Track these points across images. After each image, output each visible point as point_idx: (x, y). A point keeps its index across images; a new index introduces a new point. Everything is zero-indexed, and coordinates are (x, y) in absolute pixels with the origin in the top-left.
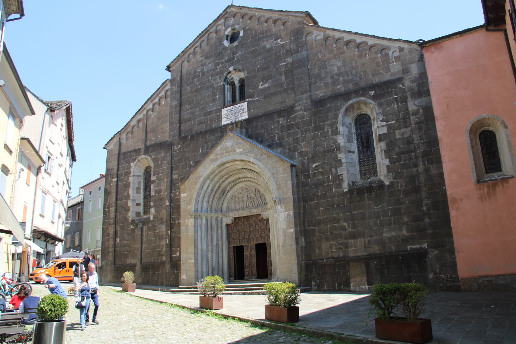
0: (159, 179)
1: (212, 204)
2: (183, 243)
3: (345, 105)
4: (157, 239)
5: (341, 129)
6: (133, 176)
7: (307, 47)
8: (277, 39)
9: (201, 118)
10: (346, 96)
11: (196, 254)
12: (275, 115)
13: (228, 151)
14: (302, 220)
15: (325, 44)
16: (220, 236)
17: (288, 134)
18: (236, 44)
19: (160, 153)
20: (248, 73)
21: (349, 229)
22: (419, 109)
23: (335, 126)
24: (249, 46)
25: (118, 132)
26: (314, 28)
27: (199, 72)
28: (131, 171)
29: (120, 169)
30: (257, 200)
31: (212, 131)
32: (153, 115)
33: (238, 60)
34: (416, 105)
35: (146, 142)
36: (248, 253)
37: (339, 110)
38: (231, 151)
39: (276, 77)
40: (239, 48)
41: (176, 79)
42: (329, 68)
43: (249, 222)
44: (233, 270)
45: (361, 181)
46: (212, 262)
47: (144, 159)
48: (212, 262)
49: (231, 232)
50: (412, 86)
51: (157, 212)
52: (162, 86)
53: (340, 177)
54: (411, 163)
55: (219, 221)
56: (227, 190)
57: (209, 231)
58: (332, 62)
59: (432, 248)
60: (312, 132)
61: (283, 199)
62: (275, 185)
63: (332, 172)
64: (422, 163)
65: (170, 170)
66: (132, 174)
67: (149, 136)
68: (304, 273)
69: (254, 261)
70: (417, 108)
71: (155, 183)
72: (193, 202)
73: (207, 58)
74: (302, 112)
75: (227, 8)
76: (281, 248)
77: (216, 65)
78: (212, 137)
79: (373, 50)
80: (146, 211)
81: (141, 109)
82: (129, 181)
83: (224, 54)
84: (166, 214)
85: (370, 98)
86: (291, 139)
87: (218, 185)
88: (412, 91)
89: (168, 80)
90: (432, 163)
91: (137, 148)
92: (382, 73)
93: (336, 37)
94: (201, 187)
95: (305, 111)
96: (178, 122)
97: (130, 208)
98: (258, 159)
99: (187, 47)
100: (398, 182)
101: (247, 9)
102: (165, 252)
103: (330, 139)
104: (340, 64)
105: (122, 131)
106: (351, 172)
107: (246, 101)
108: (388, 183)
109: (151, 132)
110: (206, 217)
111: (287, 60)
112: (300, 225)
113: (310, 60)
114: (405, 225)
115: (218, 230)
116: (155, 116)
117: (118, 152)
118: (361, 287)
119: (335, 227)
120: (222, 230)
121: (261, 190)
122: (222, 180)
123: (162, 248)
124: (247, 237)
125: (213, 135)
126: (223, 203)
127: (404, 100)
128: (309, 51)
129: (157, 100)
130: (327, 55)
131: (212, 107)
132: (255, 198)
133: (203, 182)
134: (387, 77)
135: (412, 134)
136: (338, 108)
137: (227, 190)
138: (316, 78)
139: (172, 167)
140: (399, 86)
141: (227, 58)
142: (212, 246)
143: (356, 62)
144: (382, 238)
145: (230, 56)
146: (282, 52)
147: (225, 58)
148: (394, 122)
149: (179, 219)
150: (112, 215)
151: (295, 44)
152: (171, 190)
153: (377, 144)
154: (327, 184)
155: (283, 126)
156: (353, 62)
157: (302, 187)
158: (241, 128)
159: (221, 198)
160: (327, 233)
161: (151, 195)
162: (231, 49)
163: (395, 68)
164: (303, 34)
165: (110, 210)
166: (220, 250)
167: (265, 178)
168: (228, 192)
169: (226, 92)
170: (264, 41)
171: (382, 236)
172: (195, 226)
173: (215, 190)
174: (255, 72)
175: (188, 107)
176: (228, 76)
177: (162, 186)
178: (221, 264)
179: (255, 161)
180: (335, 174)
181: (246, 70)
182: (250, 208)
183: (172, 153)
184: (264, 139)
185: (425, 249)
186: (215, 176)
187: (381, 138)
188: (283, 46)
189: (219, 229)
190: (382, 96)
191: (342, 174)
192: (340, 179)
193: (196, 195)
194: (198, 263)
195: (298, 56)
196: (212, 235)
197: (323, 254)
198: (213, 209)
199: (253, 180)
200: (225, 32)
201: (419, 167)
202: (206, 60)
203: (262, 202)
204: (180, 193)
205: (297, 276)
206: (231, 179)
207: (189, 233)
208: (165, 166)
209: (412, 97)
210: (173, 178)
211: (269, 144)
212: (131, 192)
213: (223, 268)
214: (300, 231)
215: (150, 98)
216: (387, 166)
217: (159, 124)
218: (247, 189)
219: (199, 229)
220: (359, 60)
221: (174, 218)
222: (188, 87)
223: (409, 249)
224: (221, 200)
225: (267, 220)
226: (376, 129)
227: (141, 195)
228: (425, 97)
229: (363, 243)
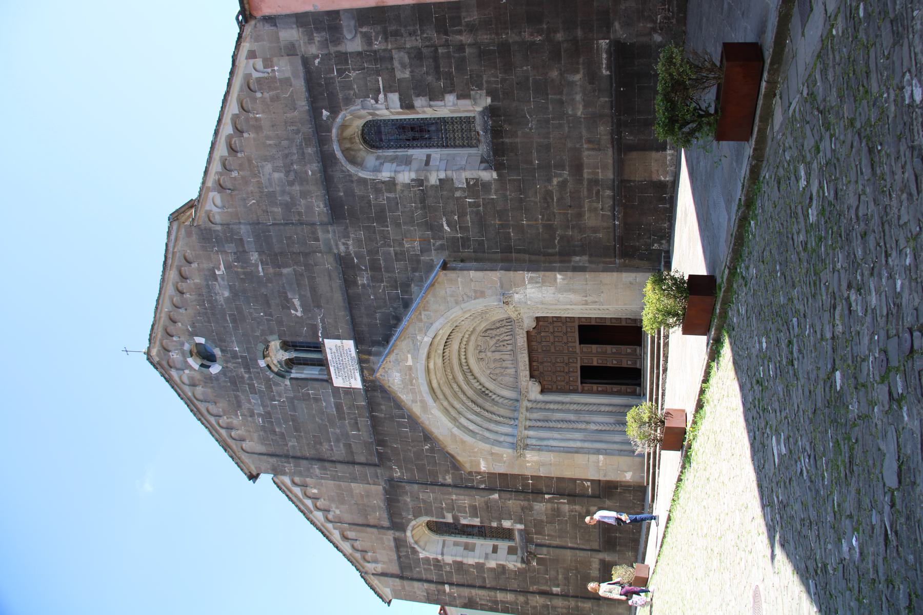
0: (451, 509)
1: (502, 417)
2: (568, 474)
3: (344, 164)
4: (559, 520)
5: (385, 175)
6: (442, 554)
7: (233, 224)
8: (214, 277)
9: (347, 424)
10: (327, 161)
11: (589, 452)
12: (350, 291)
13: (410, 381)
14: (542, 258)
15: (230, 191)
16: (560, 407)
17: (388, 270)
18: (217, 352)
19: (405, 503)
20: (272, 333)
21: (565, 176)
22: (361, 32)
23: (380, 186)
24: (224, 327)
25: (362, 577)
26: (201, 207)
27: (263, 422)
28: (433, 559)
29: (429, 577)
30: (501, 335)
31: (372, 406)
32: (336, 511)
33: (248, 350)
34: (353, 38)
35: (383, 528)
36: (595, 359)
37: (350, 176)
38: (410, 375)
39: (283, 284)
40: (225, 347)
41: (273, 465)
42: (274, 186)
43: (540, 352)
44: (623, 387)
45: (480, 147)
46: (606, 424)
47: (414, 532)
48: (606, 424)
49: (554, 386)
50: (319, 41)
51: (510, 515)
52: (284, 492)
53: (471, 183)
54: (457, 55)
55: (534, 405)
56: (480, 387)
57: (551, 424)
58: (264, 180)
59: (609, 32)
60: (388, 227)
61: (502, 287)
62: (477, 301)
63: (460, 197)
64: (457, 37)
65: (436, 487)
66: (440, 557)
67: (372, 521)
68: (637, 262)
69: (609, 349)
70: (359, 35)
71: (458, 516)
72: (496, 449)
73: (239, 406)
74: (350, 242)
75: (152, 363)
76: (589, 299)
77: (253, 390)
78: (383, 407)
79: (248, 105)
80: (506, 534)
81: (322, 533)
82: (451, 562)
83: (234, 374)
84: (515, 500)
85: (334, 119)
86: (397, 265)
87: (470, 404)
88: (327, 43)
89: (275, 479)
90: (459, 18)
91: (392, 544)
92: (292, 92)
93: (221, 170)
94: (470, 433)
95: (349, 237)
96: (351, 467)
97: (500, 565)
98: (428, 328)
99: (217, 440)
100: (488, 82)
101: (156, 326)
102: (583, 507)
103: (402, 195)
104: (268, 167)
105: (361, 569)
106: (464, 162)
107: (323, 341)
108: (489, 100)
109: (366, 517)
110: (525, 429)
111: (253, 262)
112: (550, 262)
113: (258, 220)
114: (566, 75)
115: (549, 409)
116: (337, 508)
117: (398, 580)
118: (668, 163)
119: (558, 200)
120: (550, 402)
121: (483, 326)
122: (462, 396)
123: (576, 511)
124: (566, 358)
125: (380, 404)
126: (503, 397)
127: (343, 57)
128: (242, 221)
129: (309, 502)
130: (251, 188)
131: (329, 404)
132: (497, 338)
133: (462, 429)
134: (299, 84)
135: (404, 48)
136: (348, 177)
137: (480, 387)
138: (290, 212)
139: (432, 484)
140: (317, 65)
141: (242, 370)
142: (577, 422)
143: (268, 138)
144: (584, 118)
145: (239, 363)
146: (239, 270)
147: (241, 373)
148: (380, 79)
149: (524, 478)
150: (510, 597)
151: (226, 245)
152: (472, 488)
153: (418, 113)
154: (481, 208)
155: (373, 279)
156: (269, 142)
157: (484, 252)
158: (370, 353)
159: (493, 400)
160: (569, 216)
161: (479, 524)
162: (226, 361)
163: (284, 68)
164: (210, 230)
165: (501, 601)
166: (586, 408)
167: (462, 319)
168: (484, 387)
169: (303, 376)
170: (216, 300)
171: (580, 117)
172: (540, 449)
173: (478, 409)
174: (271, 320)
175: (326, 446)
176: (276, 370)
177: (465, 503)
178: (610, 409)
179: (431, 334)
180: (465, 192)
181: (267, 337)
182: (514, 349)
183: (406, 482)
184: (393, 314)
185: (610, 45)
186: (454, 407)
187: (407, 105)
188: (228, 267)
189: (548, 406)
190: (332, 96)
191: (467, 179)
192: (474, 184)
193: (483, 444)
194: (606, 450)
195: (248, 241)
196: (558, 421)
197: (605, 224)
198: (511, 416)
199: (465, 339)
200: (195, 370)
201: (464, 42)
202: (243, 407)
203: (505, 327)
204: (479, 473)
205: (641, 274)
206: (460, 378)
207: (550, 461)
208: (429, 495)
209: (339, 44)
210: (451, 483)
211: (401, 306)
212: (471, 561)
213: (618, 405)
214: (561, 262)
215: (304, 514)
216: (458, 98)
217: (353, 502)
218: (480, 352)
219: (545, 443)
220: (265, 133)
221: (523, 485)
222: (290, 444)
223: (608, 73)
224: (497, 399)
225: (538, 319)
226: (391, 112)
227: (478, 542)
228: (340, 21)
229: (591, 153)
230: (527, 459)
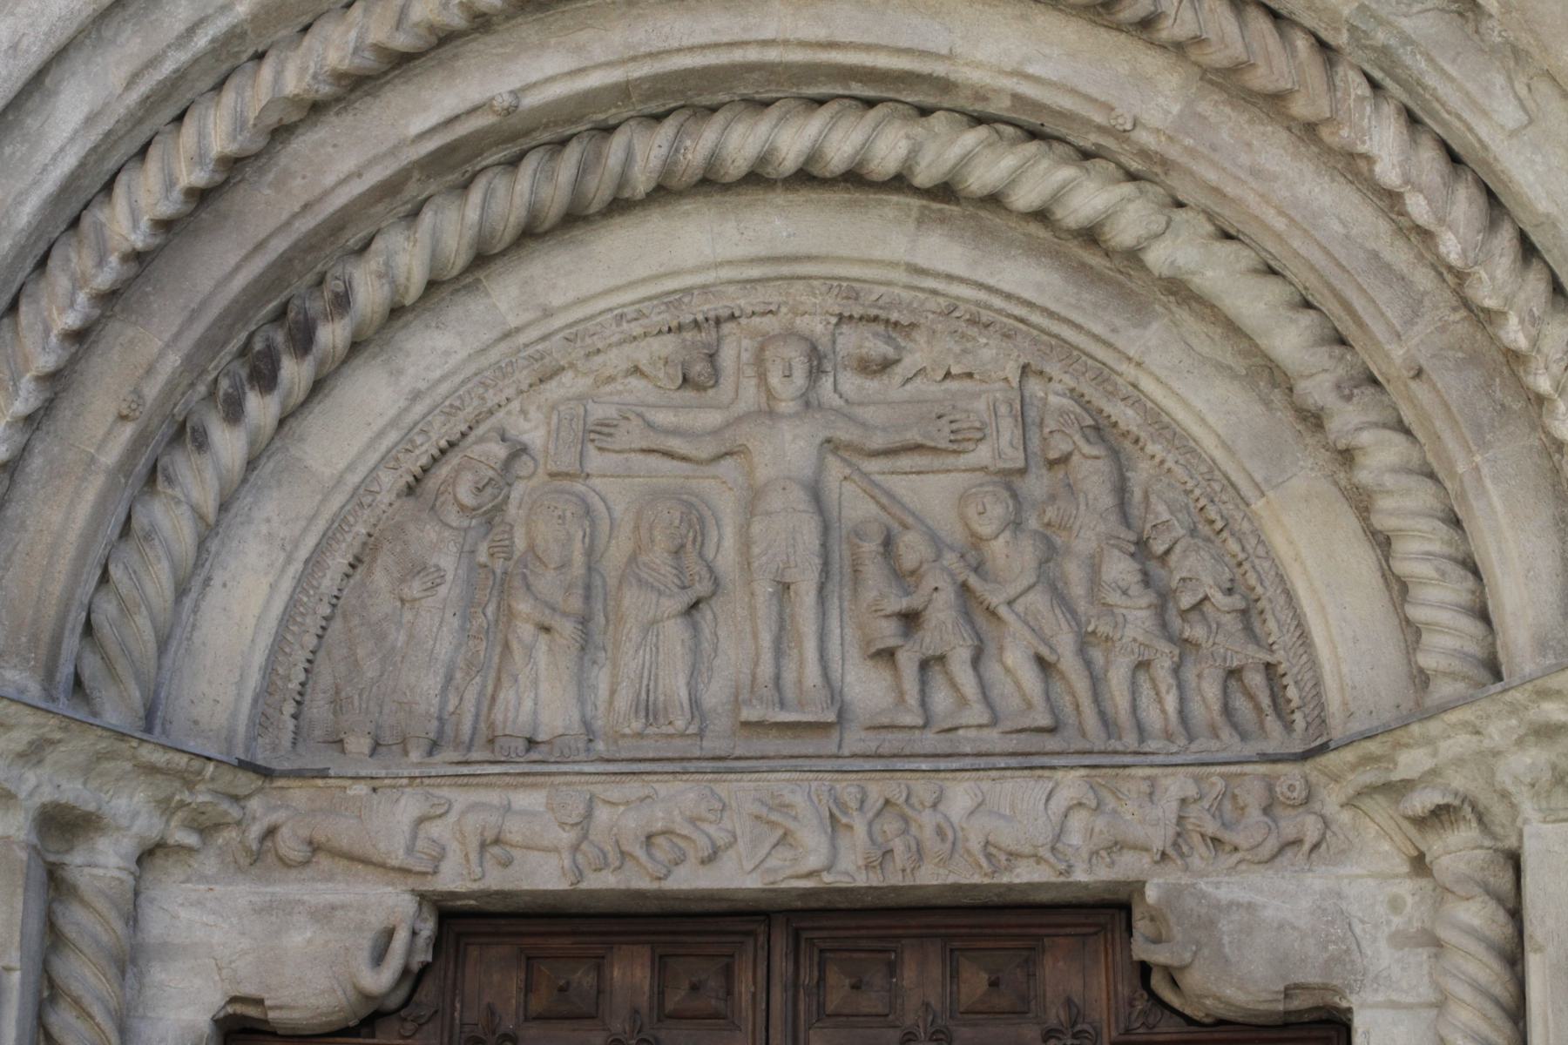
56: (369, 294)
168: (356, 346)
182: (855, 740)
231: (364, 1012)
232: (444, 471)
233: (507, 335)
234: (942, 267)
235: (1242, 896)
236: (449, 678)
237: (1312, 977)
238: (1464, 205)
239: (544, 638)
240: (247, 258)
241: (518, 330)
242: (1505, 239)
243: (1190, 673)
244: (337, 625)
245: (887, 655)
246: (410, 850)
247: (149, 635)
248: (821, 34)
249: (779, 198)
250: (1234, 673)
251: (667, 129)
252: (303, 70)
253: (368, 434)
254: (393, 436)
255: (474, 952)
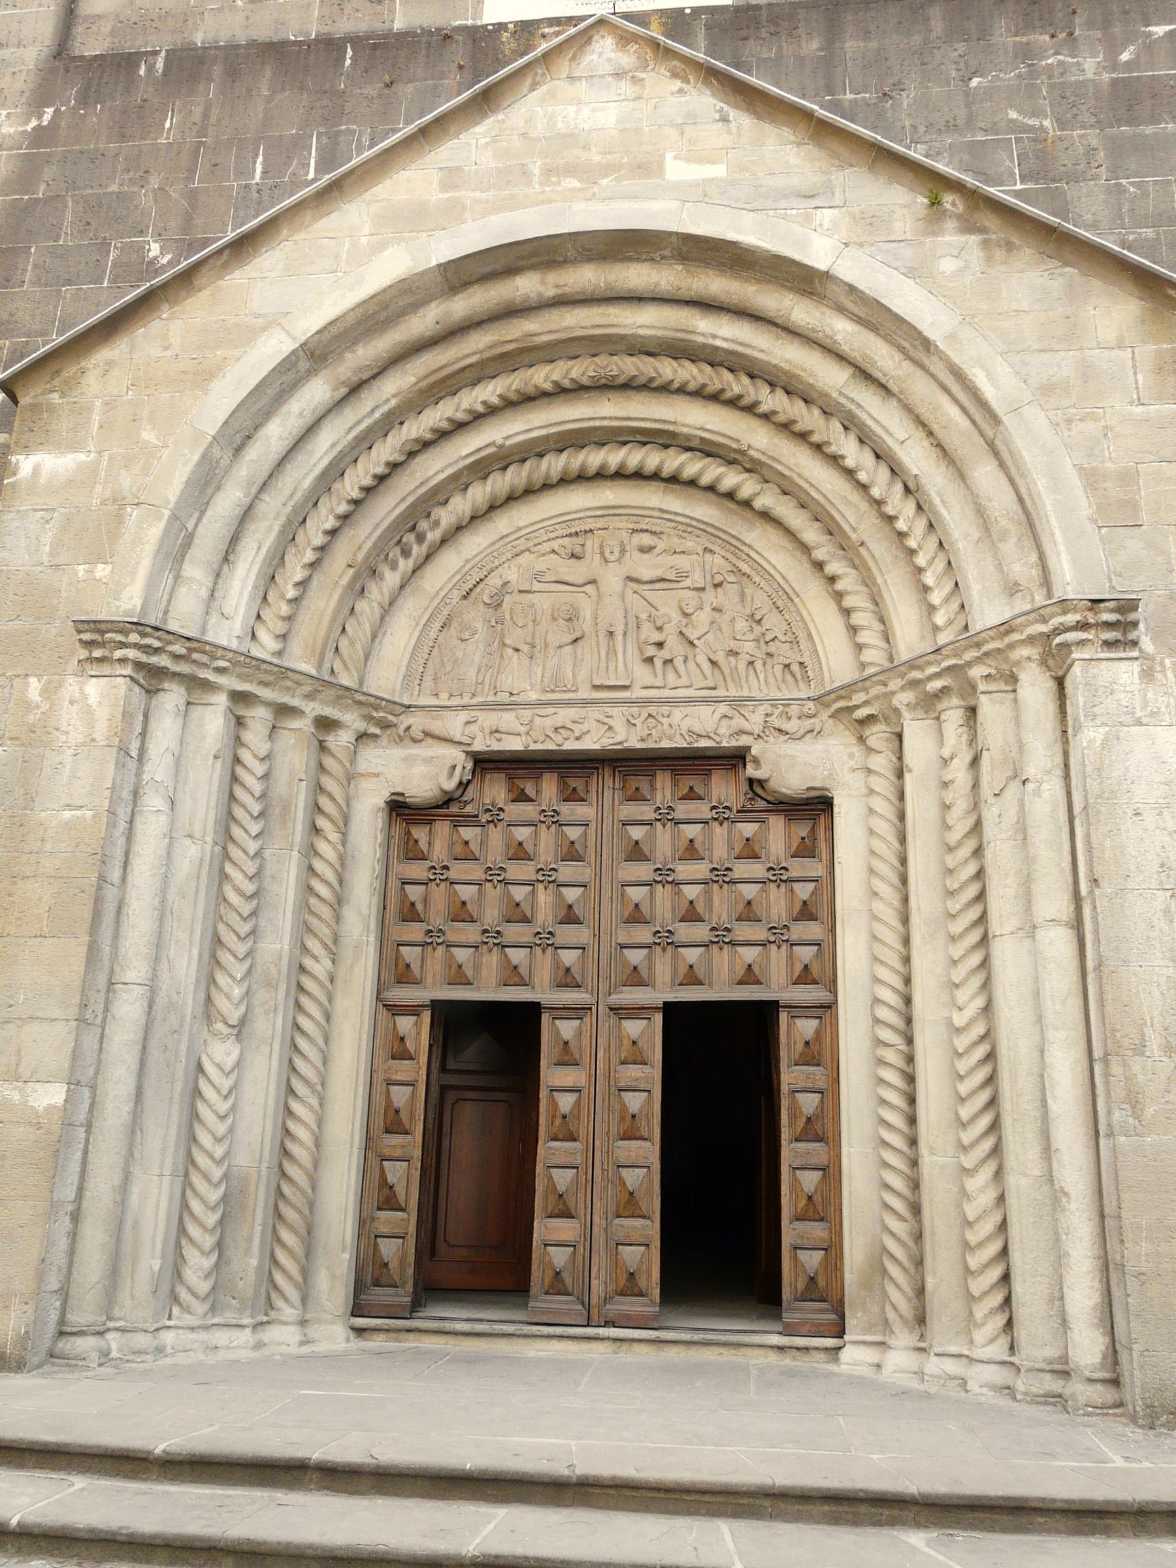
38: (607, 169)
168: (443, 541)
173: (351, 485)
230: (71, 685)
231: (445, 799)
232: (478, 590)
233: (503, 538)
234: (673, 509)
235: (790, 752)
236: (479, 670)
237: (817, 784)
238: (883, 473)
239: (516, 654)
240: (398, 504)
241: (507, 536)
242: (898, 488)
243: (769, 666)
244: (436, 650)
245: (650, 660)
246: (463, 735)
247: (361, 652)
248: (624, 414)
249: (609, 483)
250: (787, 666)
251: (565, 455)
252: (419, 428)
253: (449, 575)
254: (458, 577)
255: (488, 776)
